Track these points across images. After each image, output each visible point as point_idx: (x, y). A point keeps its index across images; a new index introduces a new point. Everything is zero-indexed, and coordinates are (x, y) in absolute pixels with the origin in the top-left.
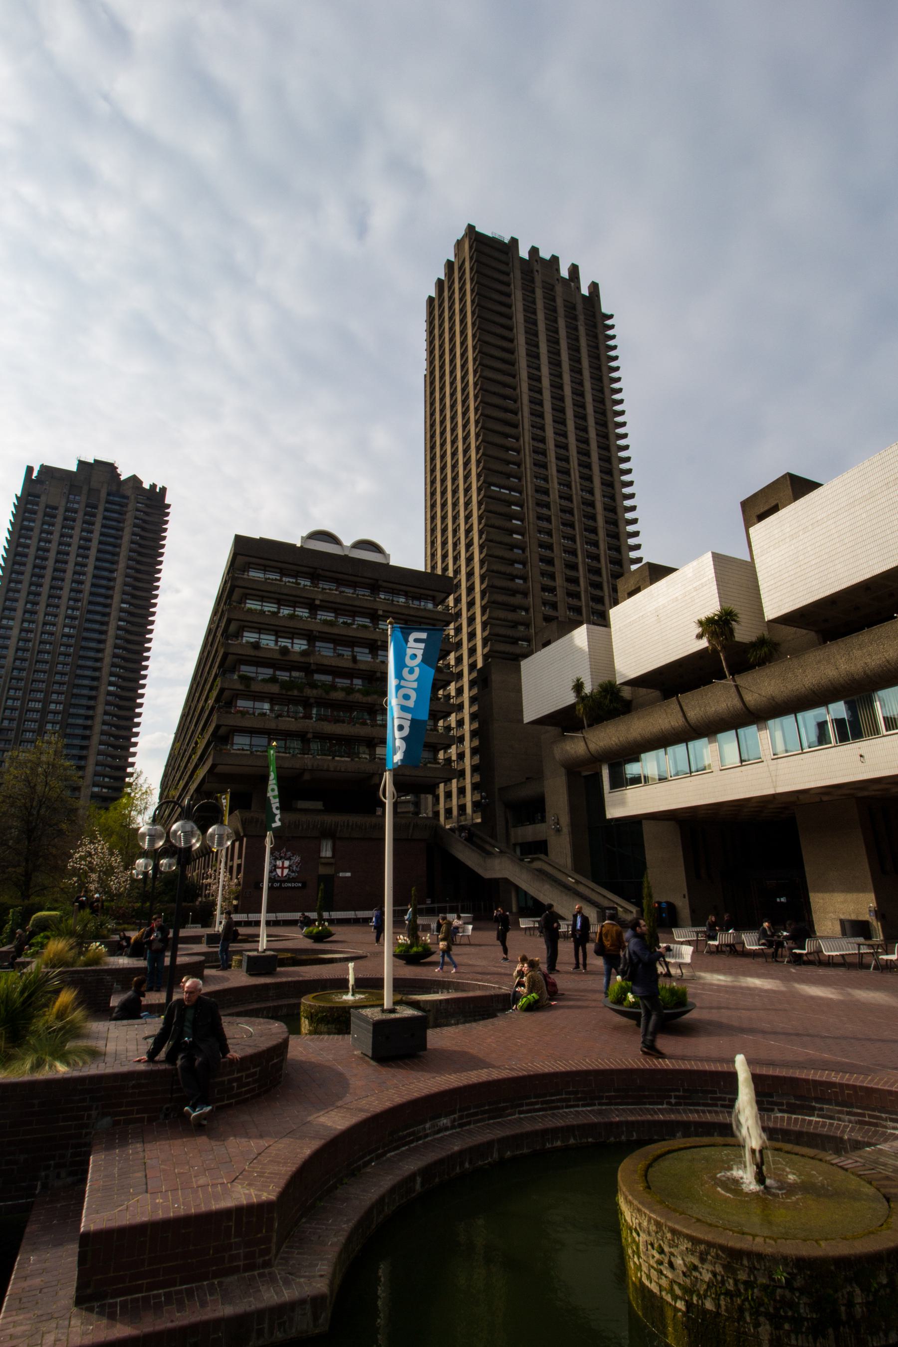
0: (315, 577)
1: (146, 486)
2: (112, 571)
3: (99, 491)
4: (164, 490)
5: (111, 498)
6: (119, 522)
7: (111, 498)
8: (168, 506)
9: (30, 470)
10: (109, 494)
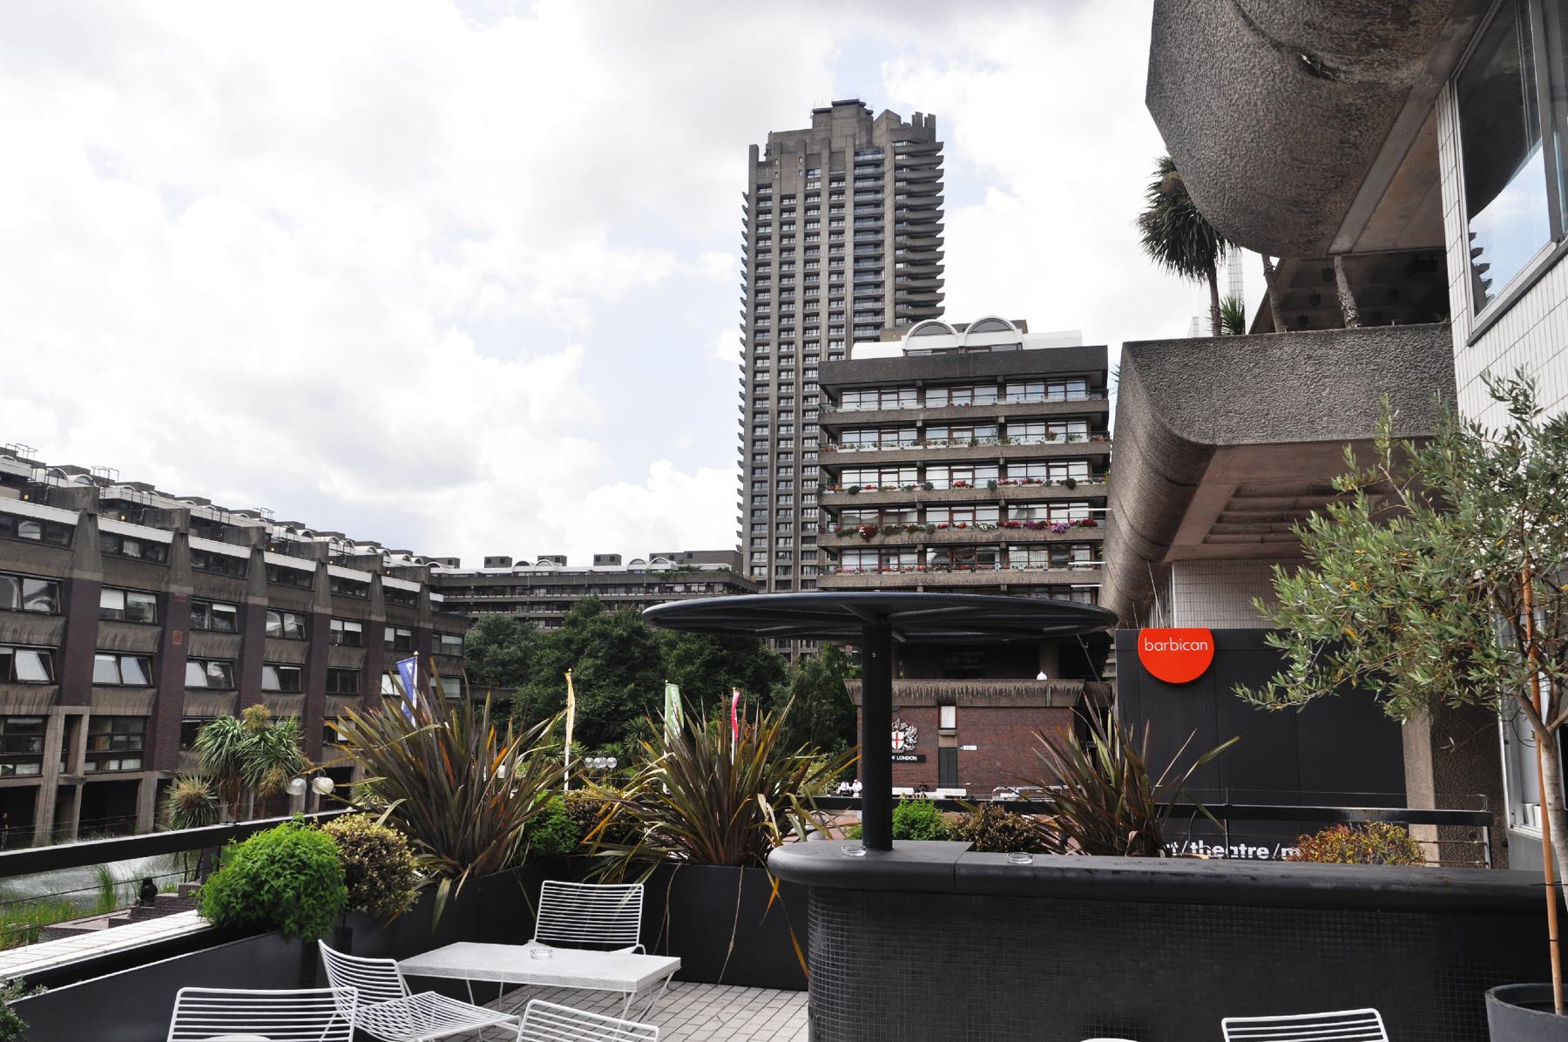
0: (923, 389)
1: (907, 119)
2: (877, 272)
3: (843, 152)
4: (931, 119)
5: (860, 158)
6: (877, 192)
7: (860, 158)
8: (940, 146)
9: (754, 150)
10: (857, 154)
